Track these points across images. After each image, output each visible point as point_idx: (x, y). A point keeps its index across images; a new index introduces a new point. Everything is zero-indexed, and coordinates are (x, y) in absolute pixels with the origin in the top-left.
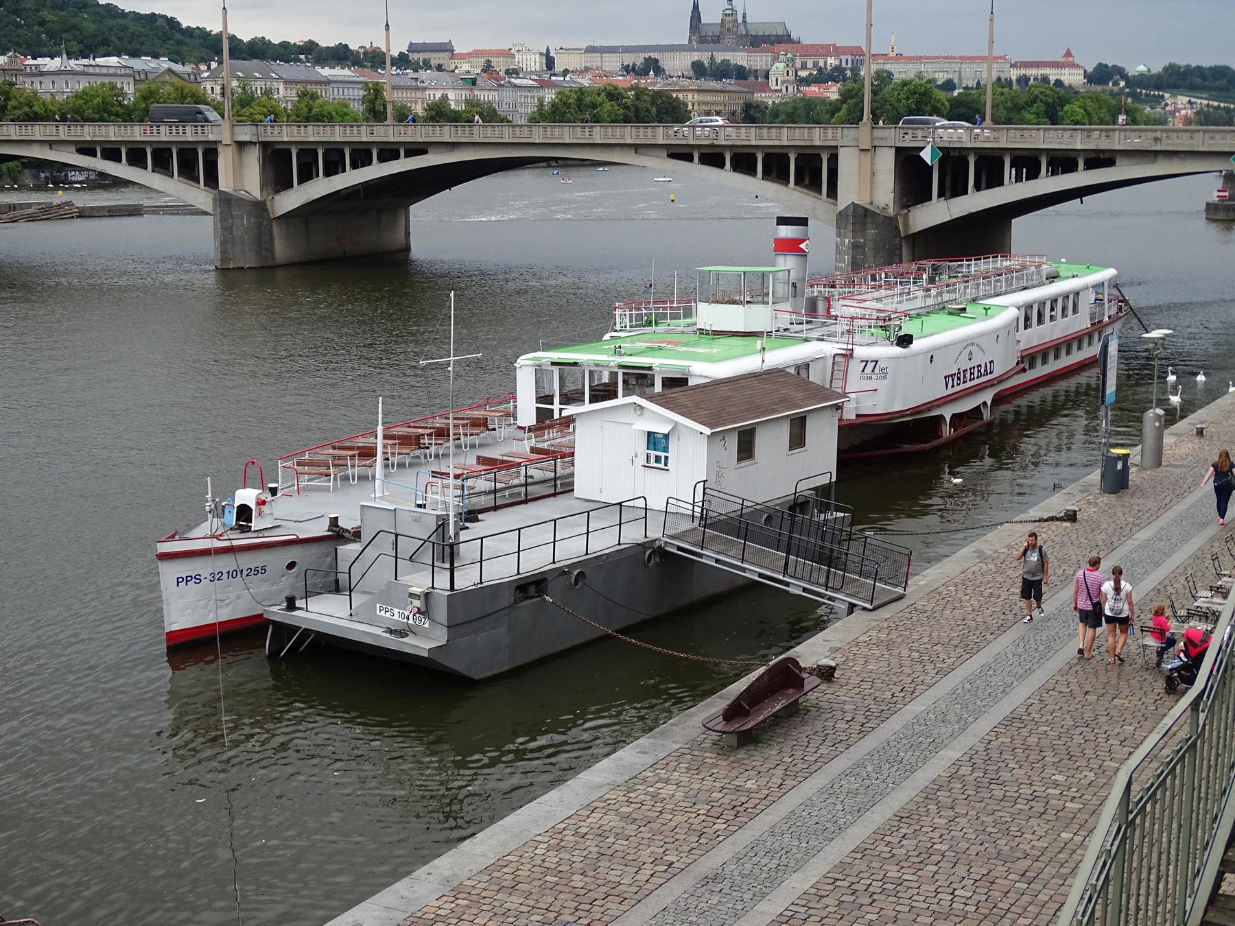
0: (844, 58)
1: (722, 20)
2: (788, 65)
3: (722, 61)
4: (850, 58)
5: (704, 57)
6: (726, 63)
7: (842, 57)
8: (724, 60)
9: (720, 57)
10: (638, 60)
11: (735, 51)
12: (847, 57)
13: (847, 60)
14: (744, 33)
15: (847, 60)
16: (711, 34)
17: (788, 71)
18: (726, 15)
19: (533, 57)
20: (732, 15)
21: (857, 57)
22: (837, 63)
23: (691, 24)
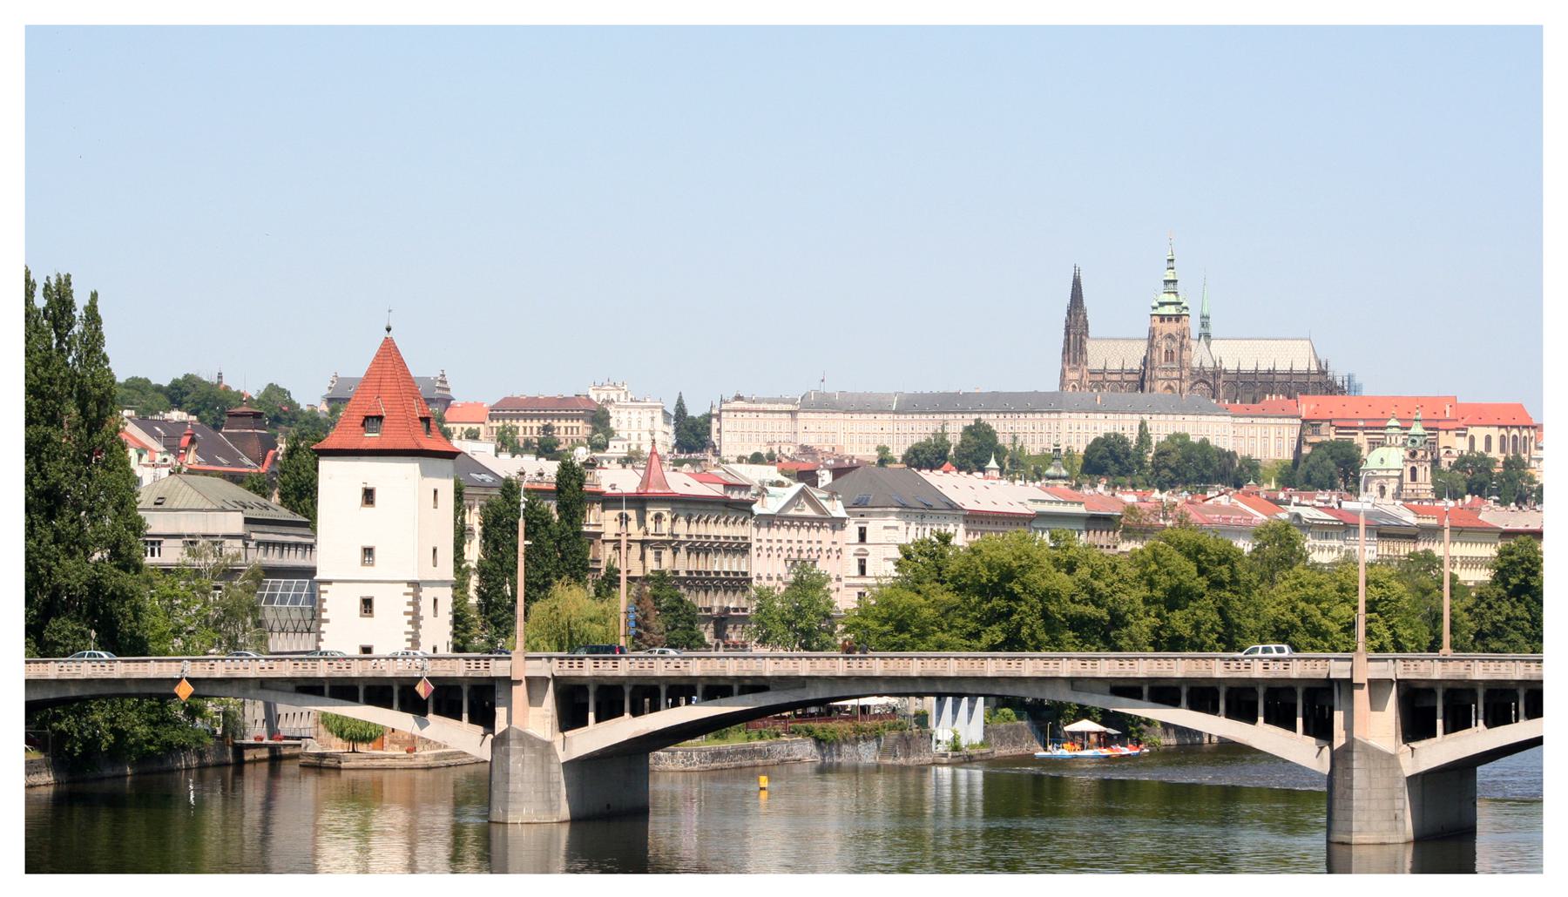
0: (1479, 433)
1: (1152, 331)
2: (1413, 454)
3: (1171, 438)
4: (1495, 433)
5: (1126, 426)
6: (1180, 440)
7: (1471, 431)
8: (1176, 435)
9: (1162, 428)
10: (955, 428)
11: (1200, 411)
12: (1485, 431)
13: (1488, 439)
14: (1208, 364)
15: (1488, 439)
16: (1117, 367)
17: (1413, 470)
18: (1162, 318)
19: (646, 415)
20: (1178, 318)
21: (1515, 432)
22: (1461, 445)
23: (1067, 341)
